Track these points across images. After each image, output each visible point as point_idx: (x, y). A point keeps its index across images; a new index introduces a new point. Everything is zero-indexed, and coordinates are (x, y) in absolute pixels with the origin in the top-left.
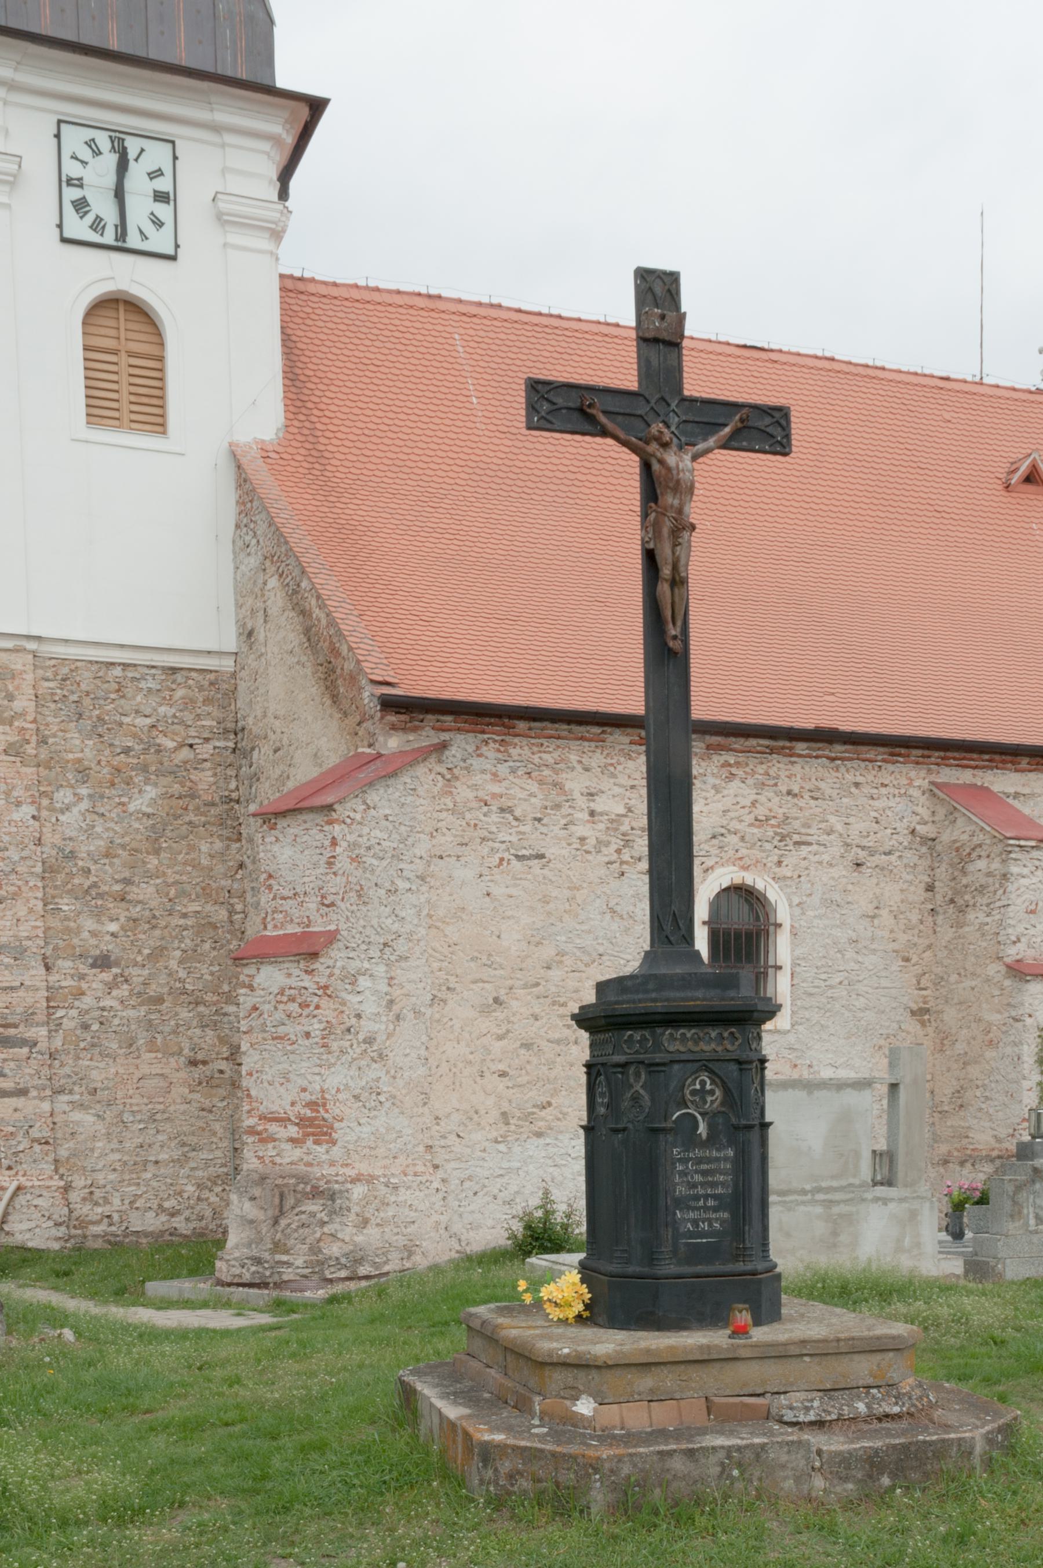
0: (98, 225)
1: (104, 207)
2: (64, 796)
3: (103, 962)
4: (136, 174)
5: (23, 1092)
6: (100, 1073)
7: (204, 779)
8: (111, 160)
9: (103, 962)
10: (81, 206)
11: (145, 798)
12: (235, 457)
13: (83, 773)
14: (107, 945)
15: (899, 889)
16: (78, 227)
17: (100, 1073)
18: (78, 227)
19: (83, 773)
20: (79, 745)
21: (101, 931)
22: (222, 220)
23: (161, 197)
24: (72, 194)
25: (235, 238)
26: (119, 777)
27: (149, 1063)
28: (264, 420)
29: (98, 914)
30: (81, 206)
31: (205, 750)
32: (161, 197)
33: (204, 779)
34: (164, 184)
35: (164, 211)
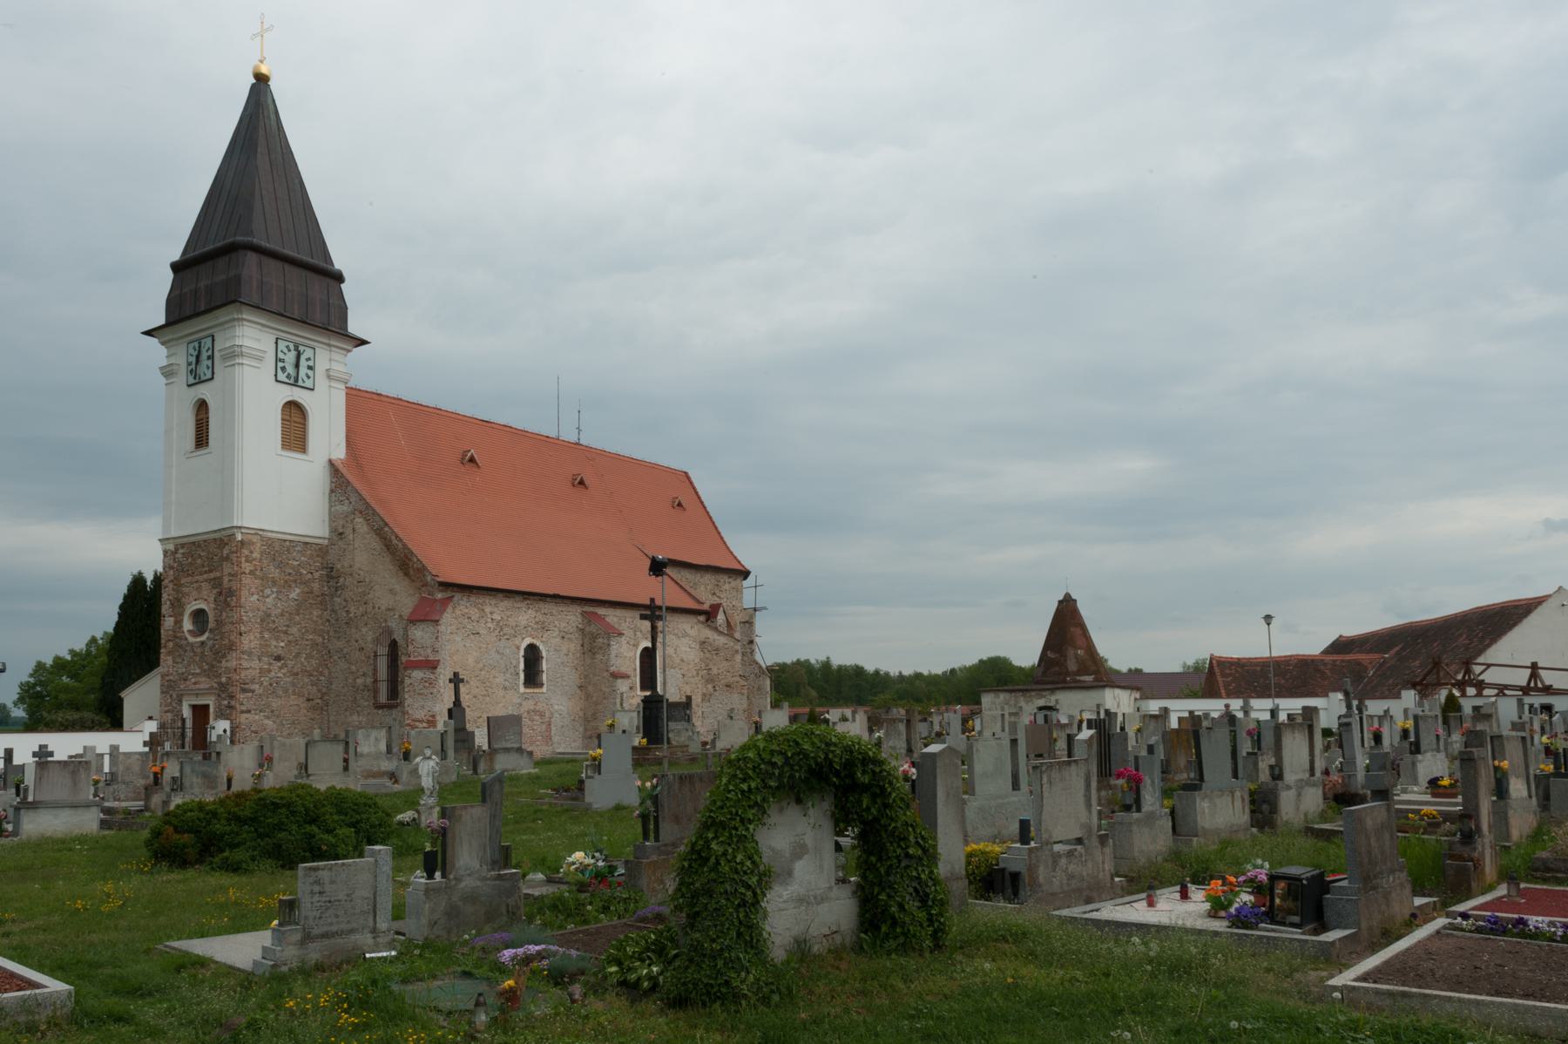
0: (288, 376)
1: (290, 370)
2: (268, 591)
3: (278, 658)
4: (303, 358)
5: (249, 711)
6: (276, 703)
7: (316, 586)
8: (293, 354)
9: (278, 658)
10: (283, 369)
11: (295, 593)
12: (331, 462)
13: (274, 582)
14: (280, 652)
15: (573, 646)
16: (282, 376)
17: (276, 703)
18: (282, 376)
19: (274, 582)
20: (274, 572)
21: (278, 646)
22: (329, 377)
23: (310, 368)
24: (280, 364)
25: (333, 384)
26: (287, 585)
27: (293, 700)
28: (340, 453)
29: (277, 639)
30: (283, 369)
31: (317, 575)
32: (310, 368)
33: (316, 586)
34: (311, 363)
35: (310, 373)
